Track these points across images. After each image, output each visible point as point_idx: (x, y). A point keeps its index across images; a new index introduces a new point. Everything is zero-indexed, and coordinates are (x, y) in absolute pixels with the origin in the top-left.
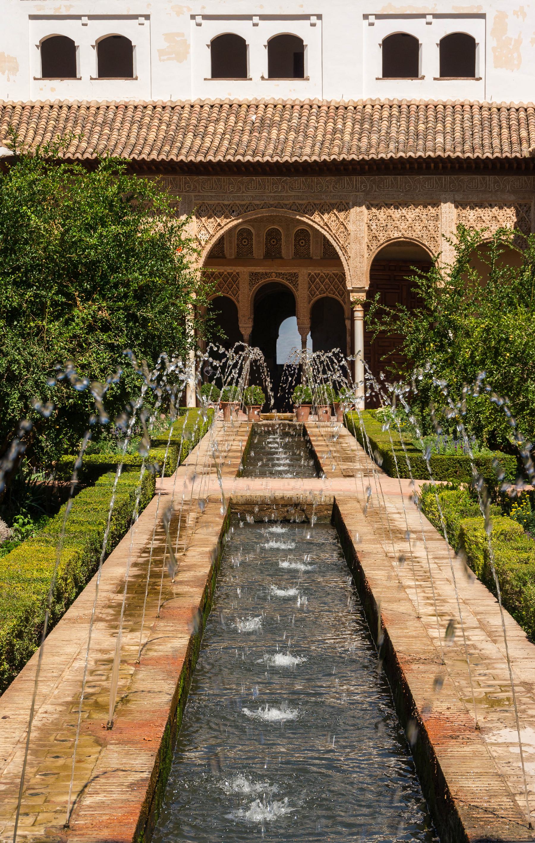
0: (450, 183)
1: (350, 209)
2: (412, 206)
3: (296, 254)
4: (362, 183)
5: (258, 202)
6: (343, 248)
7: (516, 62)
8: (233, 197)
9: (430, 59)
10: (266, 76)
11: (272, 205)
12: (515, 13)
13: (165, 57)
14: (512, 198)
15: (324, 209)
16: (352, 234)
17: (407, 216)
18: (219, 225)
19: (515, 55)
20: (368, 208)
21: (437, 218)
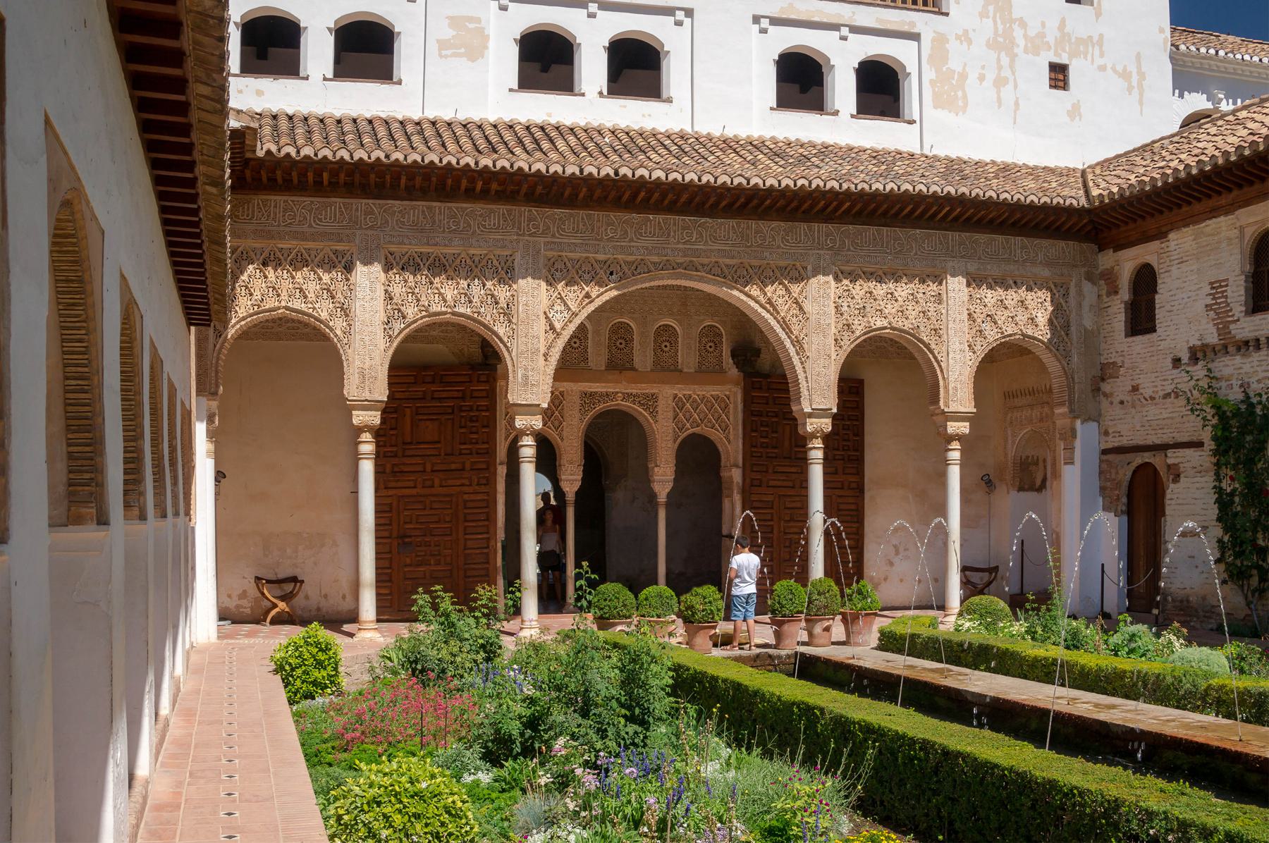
0: (960, 245)
1: (808, 279)
2: (905, 280)
3: (656, 363)
4: (827, 236)
5: (655, 259)
6: (797, 343)
7: (960, 103)
8: (614, 247)
9: (843, 88)
10: (605, 93)
11: (679, 265)
12: (958, 37)
13: (449, 52)
14: (1046, 272)
15: (765, 276)
16: (813, 318)
17: (896, 294)
18: (587, 296)
19: (960, 93)
20: (837, 279)
21: (939, 298)
